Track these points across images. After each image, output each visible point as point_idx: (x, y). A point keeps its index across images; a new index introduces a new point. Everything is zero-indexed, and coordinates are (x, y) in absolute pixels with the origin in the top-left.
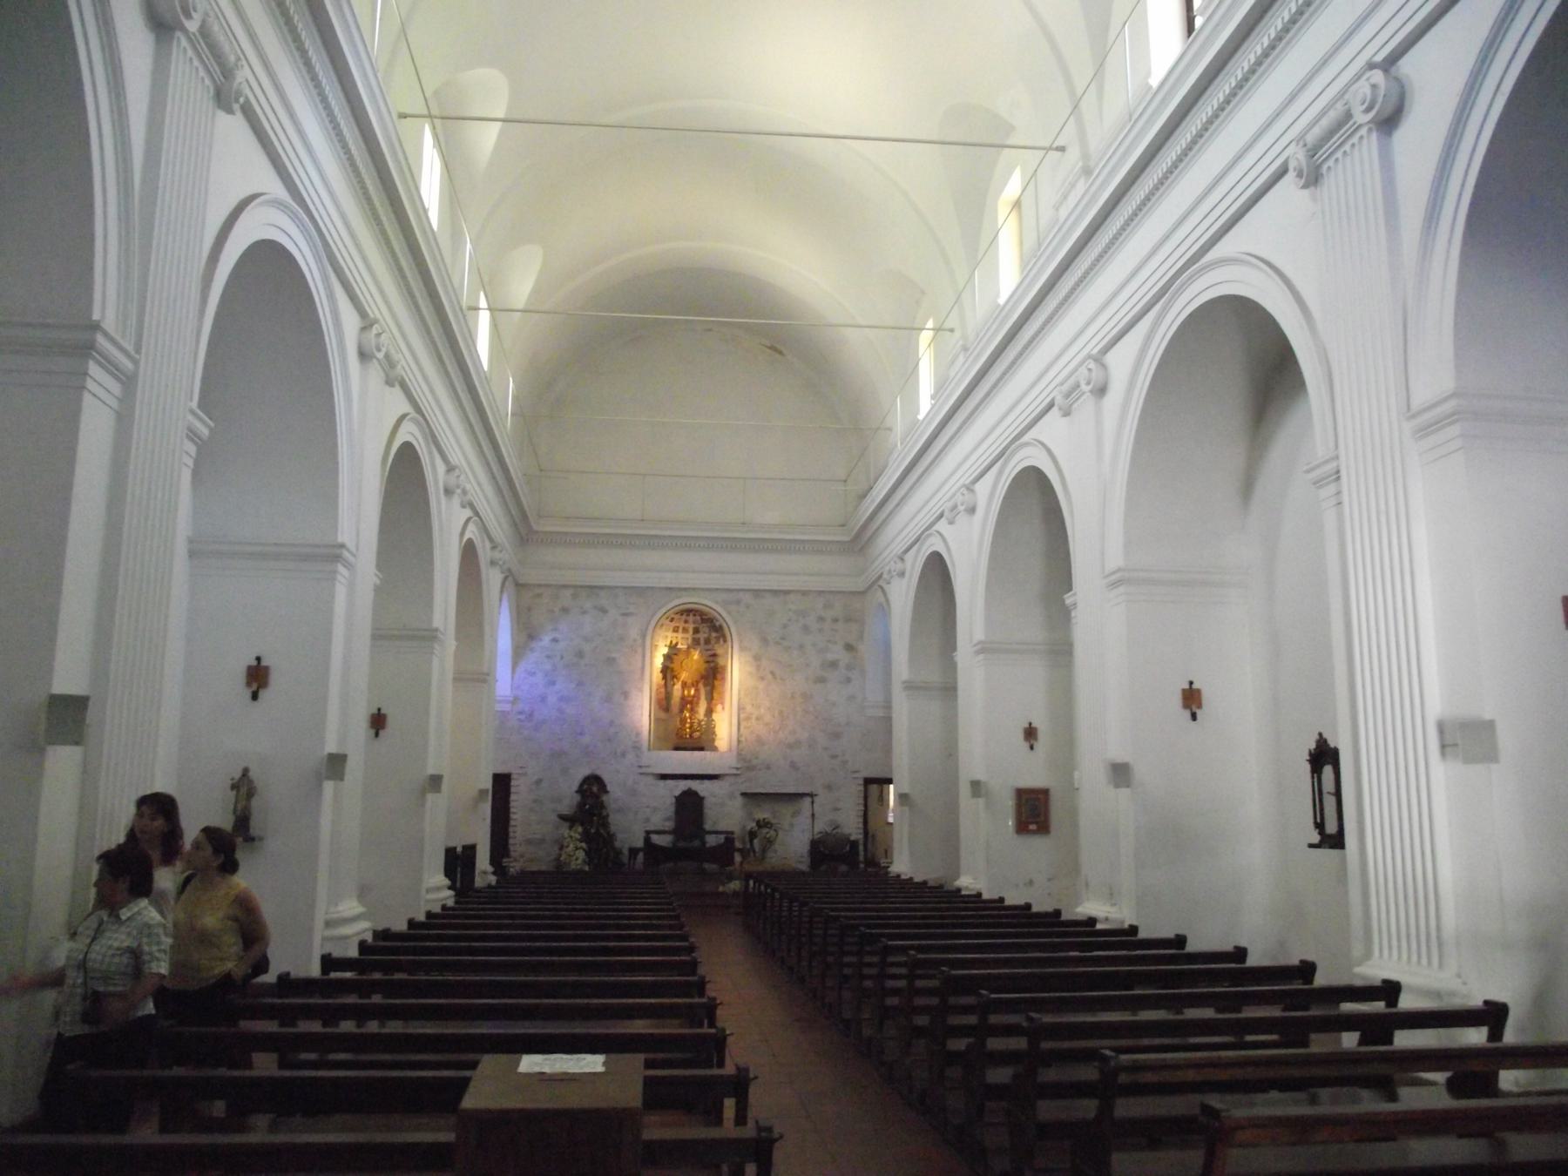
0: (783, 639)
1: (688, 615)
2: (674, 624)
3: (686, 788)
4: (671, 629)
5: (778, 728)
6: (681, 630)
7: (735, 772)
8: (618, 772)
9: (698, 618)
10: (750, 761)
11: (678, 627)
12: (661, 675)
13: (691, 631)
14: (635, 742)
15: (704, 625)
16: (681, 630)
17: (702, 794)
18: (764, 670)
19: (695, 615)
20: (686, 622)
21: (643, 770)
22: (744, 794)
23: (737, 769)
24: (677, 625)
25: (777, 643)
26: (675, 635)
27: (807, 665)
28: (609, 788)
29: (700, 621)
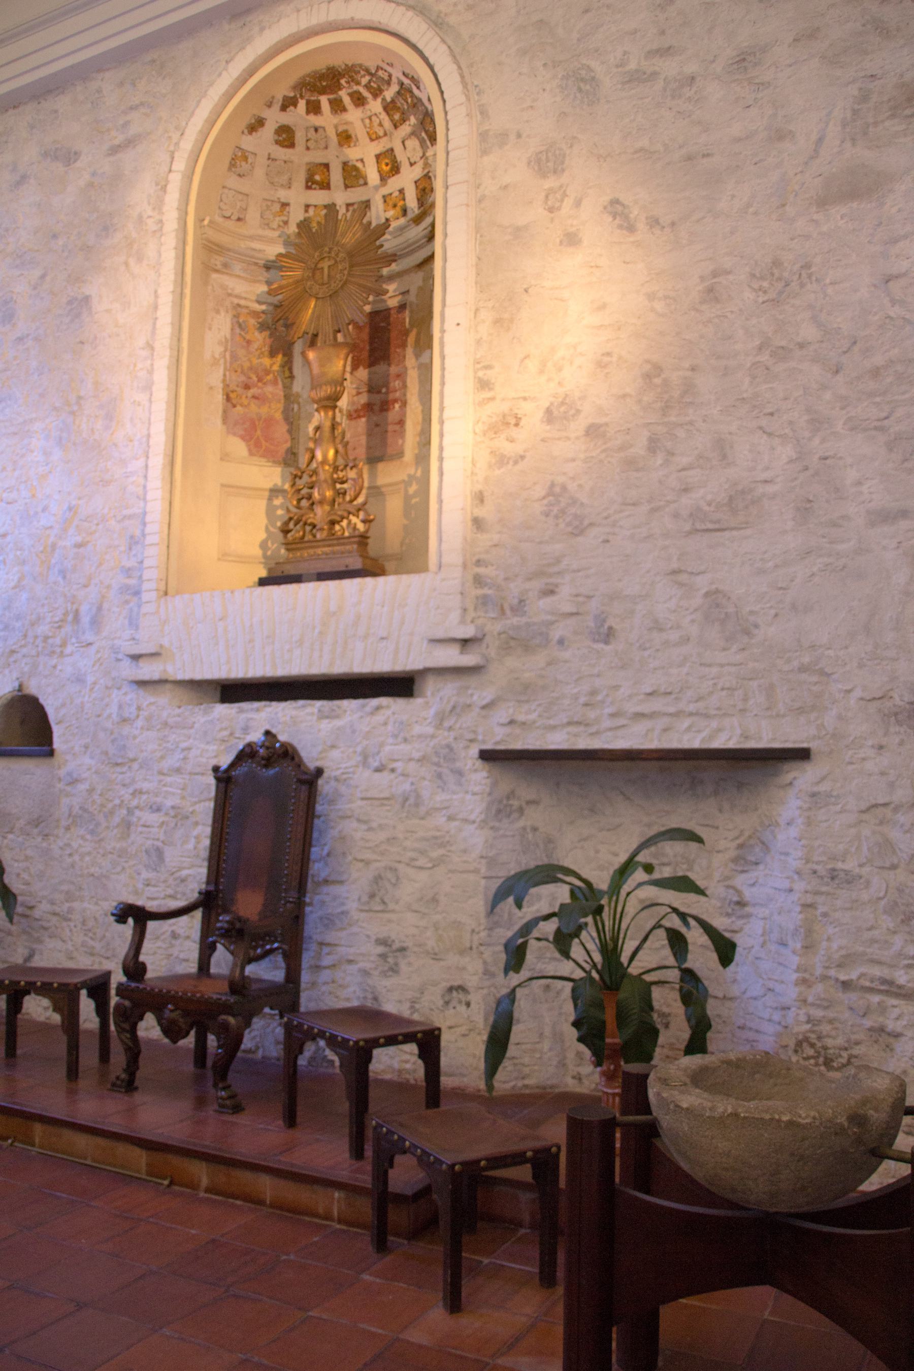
0: (666, 52)
1: (338, 107)
2: (300, 157)
3: (256, 736)
4: (301, 178)
5: (639, 448)
6: (336, 176)
7: (451, 656)
8: (79, 679)
9: (375, 106)
10: (519, 607)
11: (327, 166)
12: (260, 339)
13: (372, 175)
14: (128, 572)
15: (405, 129)
16: (336, 176)
17: (310, 757)
18: (578, 203)
19: (359, 101)
20: (346, 138)
21: (149, 670)
22: (487, 756)
23: (465, 642)
24: (318, 157)
25: (636, 78)
26: (319, 197)
27: (780, 135)
28: (57, 743)
29: (387, 124)
